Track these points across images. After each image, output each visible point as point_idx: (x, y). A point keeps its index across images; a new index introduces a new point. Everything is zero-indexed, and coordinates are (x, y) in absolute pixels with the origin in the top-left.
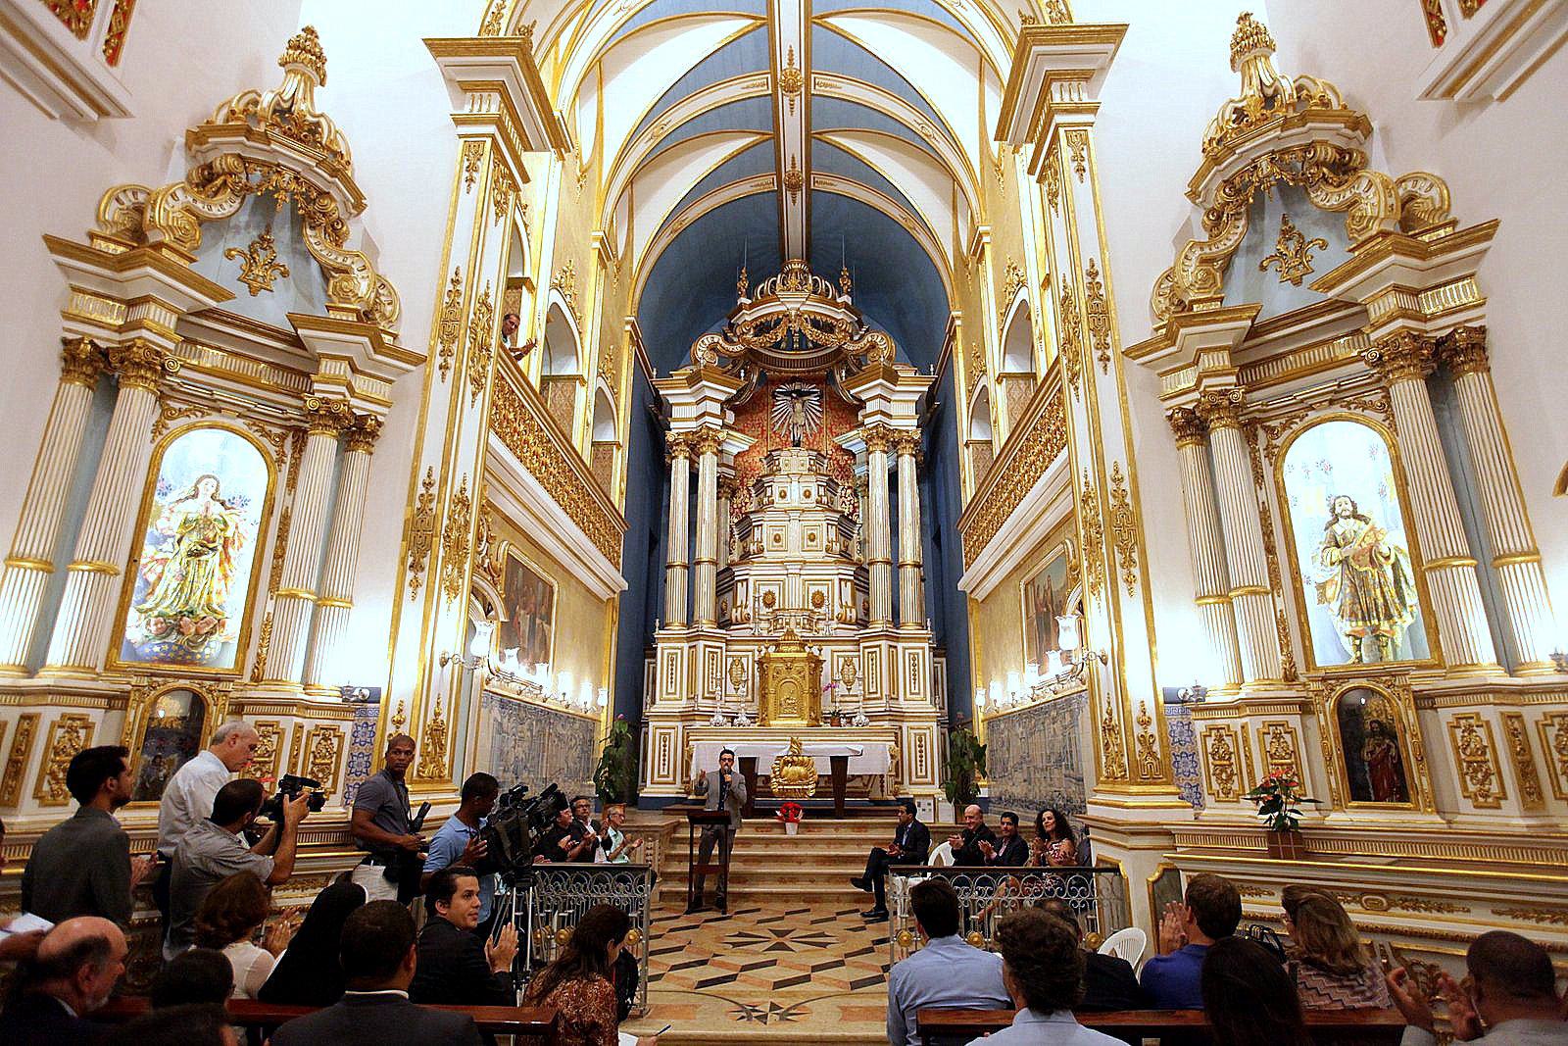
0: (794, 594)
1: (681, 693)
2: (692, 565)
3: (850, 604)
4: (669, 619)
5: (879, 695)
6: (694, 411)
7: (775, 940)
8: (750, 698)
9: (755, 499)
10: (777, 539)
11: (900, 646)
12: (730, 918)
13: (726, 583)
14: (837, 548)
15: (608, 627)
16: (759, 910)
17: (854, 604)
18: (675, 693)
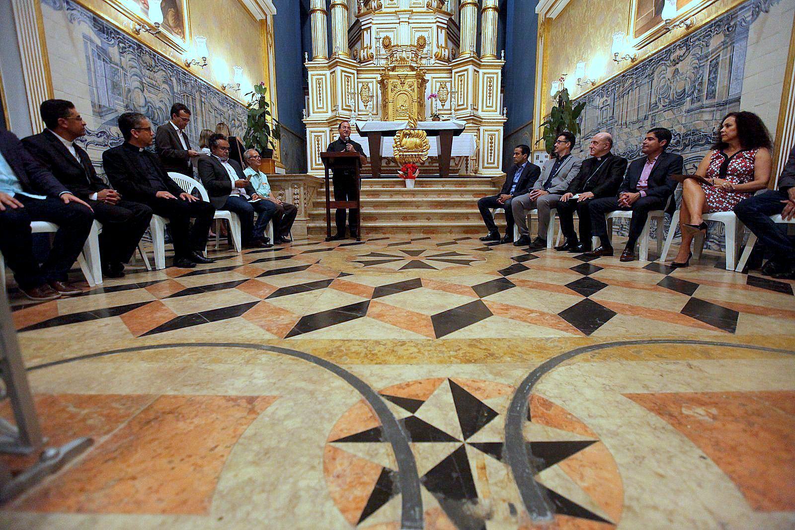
0: (404, 36)
1: (327, 107)
3: (443, 45)
5: (465, 106)
7: (409, 259)
8: (375, 112)
11: (481, 71)
12: (364, 243)
13: (355, 34)
15: (264, 45)
16: (388, 238)
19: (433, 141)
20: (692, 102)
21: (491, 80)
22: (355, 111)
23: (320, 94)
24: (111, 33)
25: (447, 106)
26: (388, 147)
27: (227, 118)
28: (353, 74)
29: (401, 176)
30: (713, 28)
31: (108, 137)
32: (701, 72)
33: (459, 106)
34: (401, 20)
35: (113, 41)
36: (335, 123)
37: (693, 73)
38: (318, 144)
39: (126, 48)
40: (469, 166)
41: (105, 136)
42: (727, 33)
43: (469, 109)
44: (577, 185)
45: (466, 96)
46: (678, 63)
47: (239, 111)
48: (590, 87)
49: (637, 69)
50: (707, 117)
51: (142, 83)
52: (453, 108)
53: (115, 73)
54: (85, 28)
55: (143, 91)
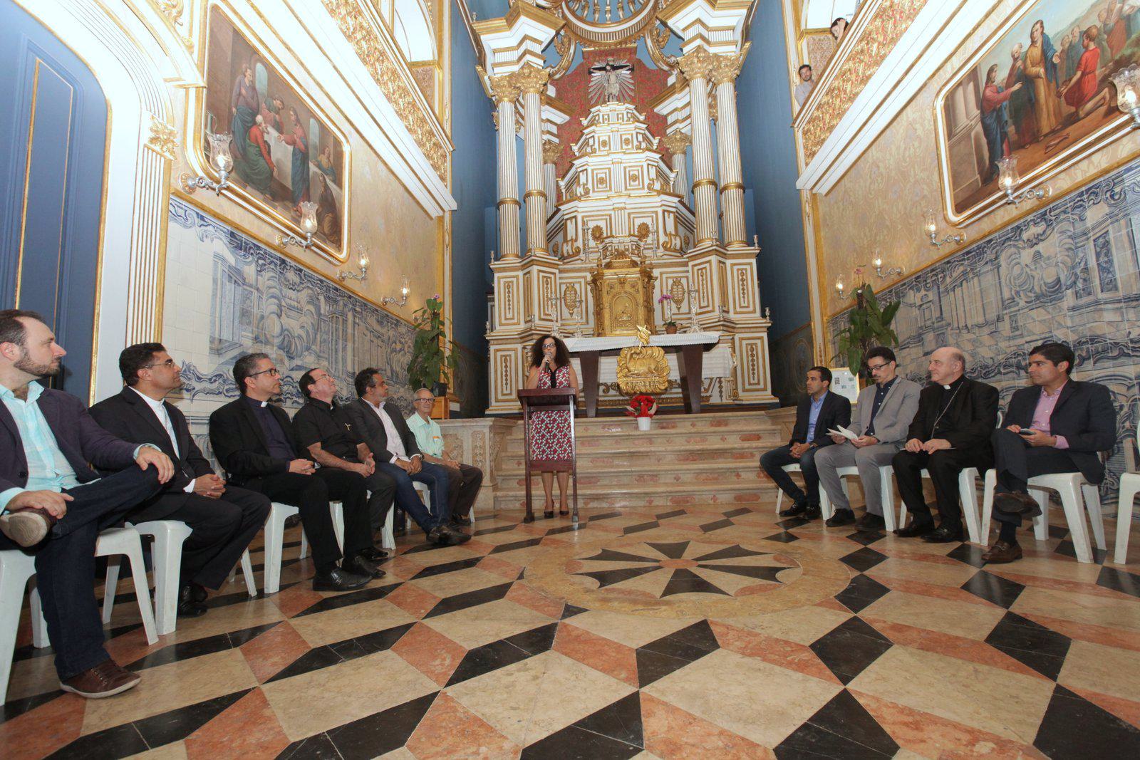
3: (673, 233)
4: (504, 251)
5: (710, 308)
11: (728, 262)
18: (513, 319)
19: (672, 361)
20: (1077, 295)
21: (742, 272)
22: (557, 321)
23: (509, 301)
24: (250, 248)
25: (684, 308)
26: (608, 371)
27: (386, 341)
29: (631, 414)
30: (1085, 196)
31: (224, 381)
32: (1081, 255)
33: (701, 308)
34: (616, 206)
35: (251, 258)
36: (530, 338)
37: (1068, 256)
38: (506, 366)
39: (265, 265)
40: (723, 390)
41: (221, 381)
42: (1113, 202)
43: (717, 313)
44: (920, 428)
45: (710, 297)
46: (1036, 244)
47: (403, 330)
48: (896, 278)
49: (968, 253)
50: (1109, 316)
51: (280, 306)
52: (694, 311)
53: (246, 297)
54: (220, 246)
55: (279, 316)
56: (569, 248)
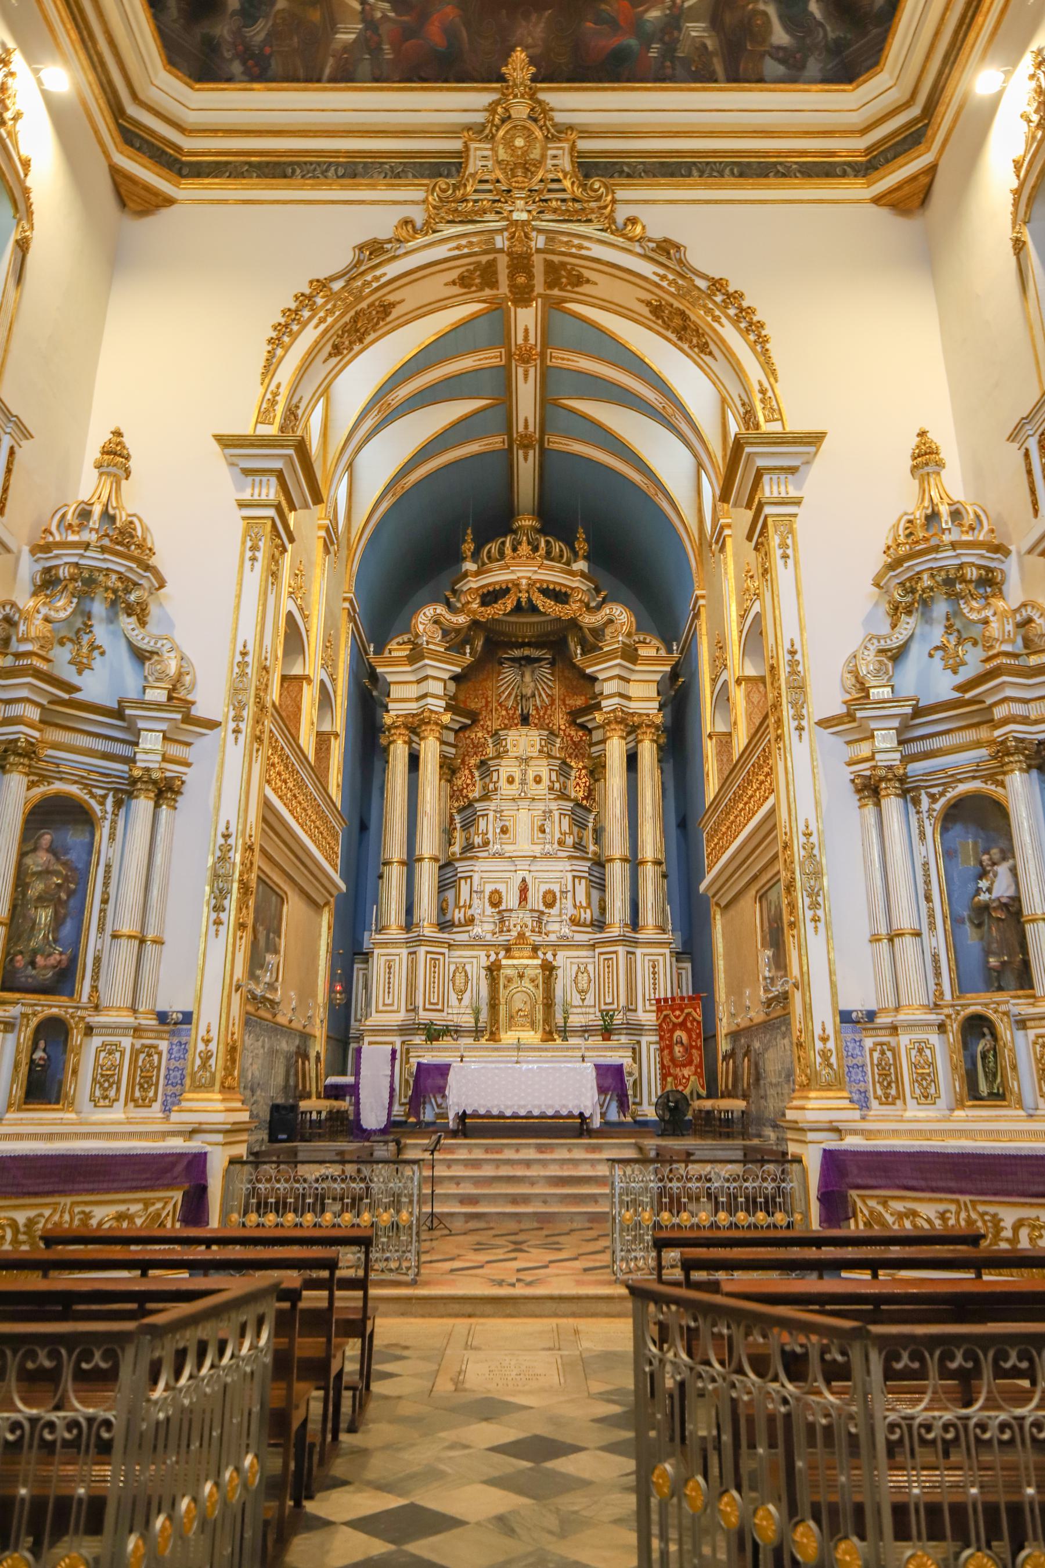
2: (411, 862)
3: (584, 904)
6: (413, 691)
9: (479, 785)
10: (504, 831)
11: (639, 951)
13: (447, 882)
14: (570, 840)
17: (589, 904)
18: (392, 1005)
28: (443, 954)
56: (462, 915)
